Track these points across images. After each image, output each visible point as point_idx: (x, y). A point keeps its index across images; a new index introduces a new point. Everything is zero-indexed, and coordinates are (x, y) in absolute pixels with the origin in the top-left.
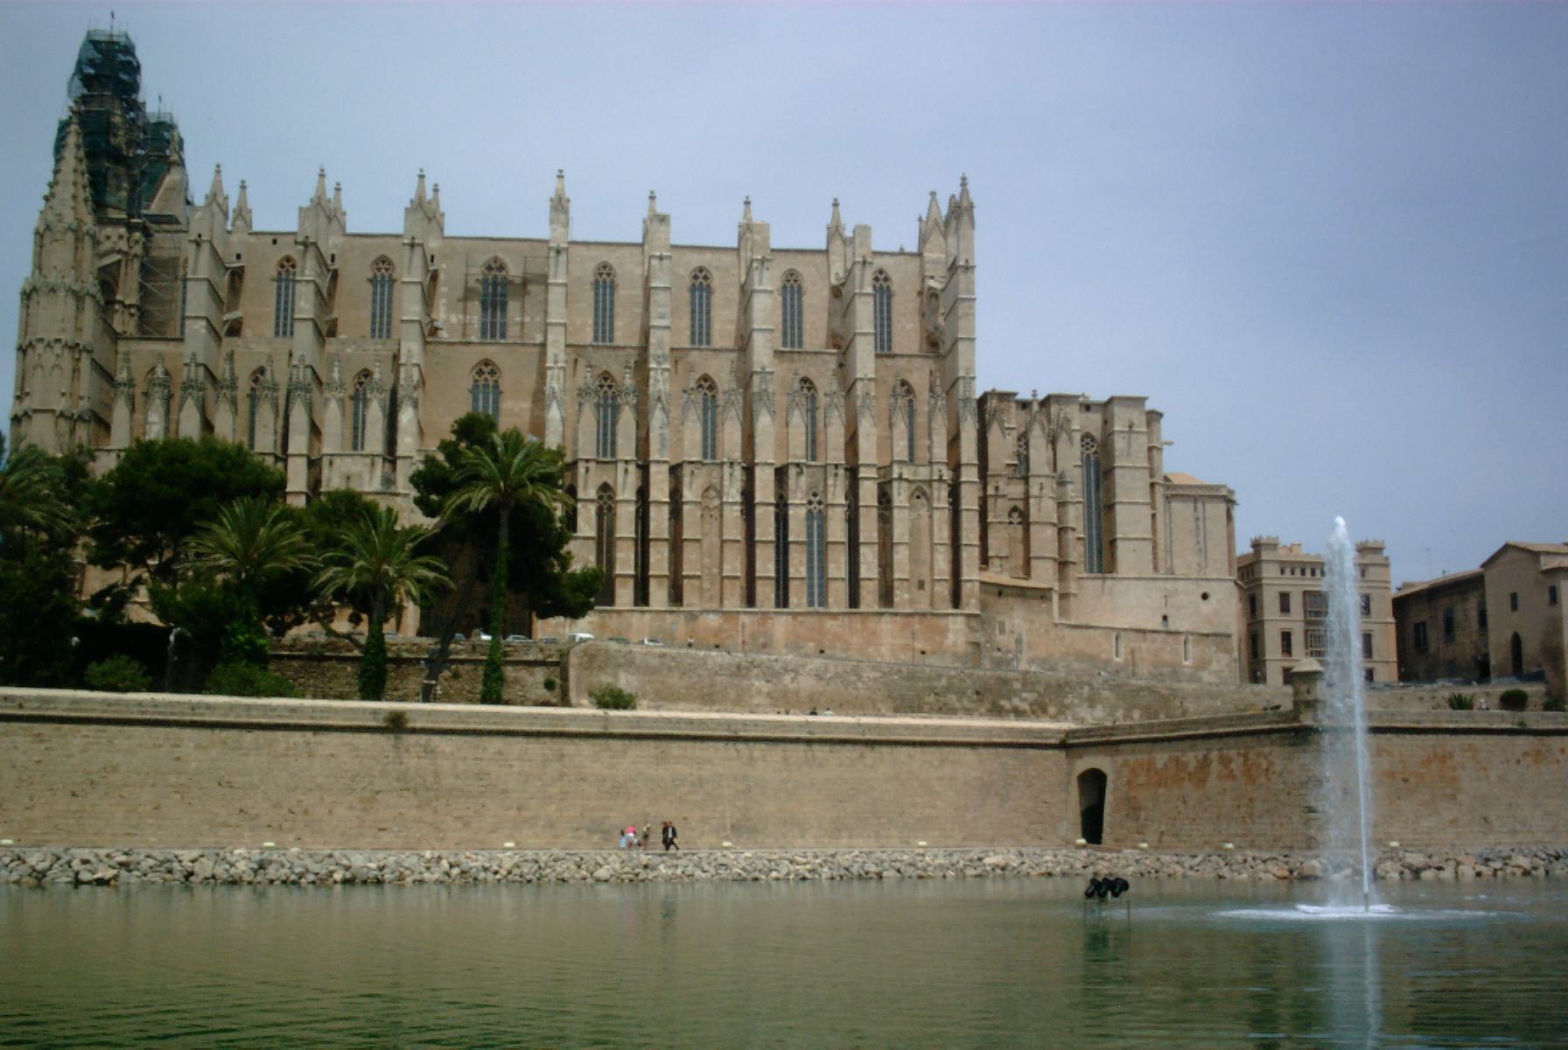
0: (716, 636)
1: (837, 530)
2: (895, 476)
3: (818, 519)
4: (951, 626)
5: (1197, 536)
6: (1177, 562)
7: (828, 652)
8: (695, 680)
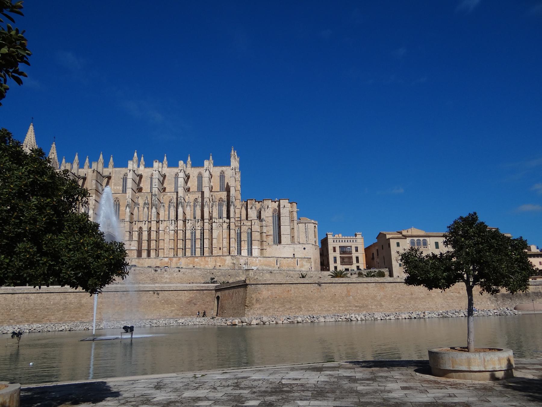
0: (167, 264)
1: (198, 236)
2: (213, 222)
3: (193, 234)
4: (227, 259)
5: (306, 233)
6: (300, 240)
7: (195, 267)
8: (148, 275)
